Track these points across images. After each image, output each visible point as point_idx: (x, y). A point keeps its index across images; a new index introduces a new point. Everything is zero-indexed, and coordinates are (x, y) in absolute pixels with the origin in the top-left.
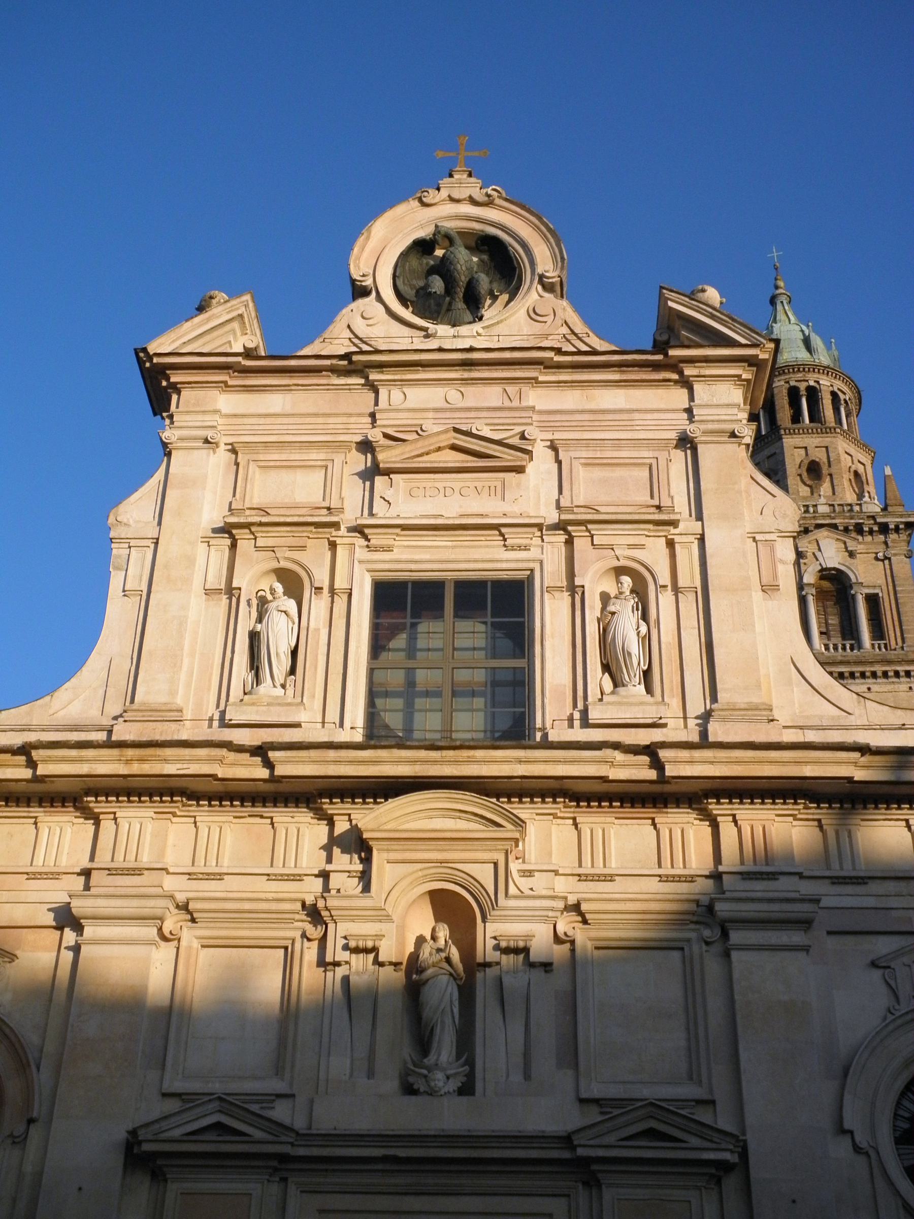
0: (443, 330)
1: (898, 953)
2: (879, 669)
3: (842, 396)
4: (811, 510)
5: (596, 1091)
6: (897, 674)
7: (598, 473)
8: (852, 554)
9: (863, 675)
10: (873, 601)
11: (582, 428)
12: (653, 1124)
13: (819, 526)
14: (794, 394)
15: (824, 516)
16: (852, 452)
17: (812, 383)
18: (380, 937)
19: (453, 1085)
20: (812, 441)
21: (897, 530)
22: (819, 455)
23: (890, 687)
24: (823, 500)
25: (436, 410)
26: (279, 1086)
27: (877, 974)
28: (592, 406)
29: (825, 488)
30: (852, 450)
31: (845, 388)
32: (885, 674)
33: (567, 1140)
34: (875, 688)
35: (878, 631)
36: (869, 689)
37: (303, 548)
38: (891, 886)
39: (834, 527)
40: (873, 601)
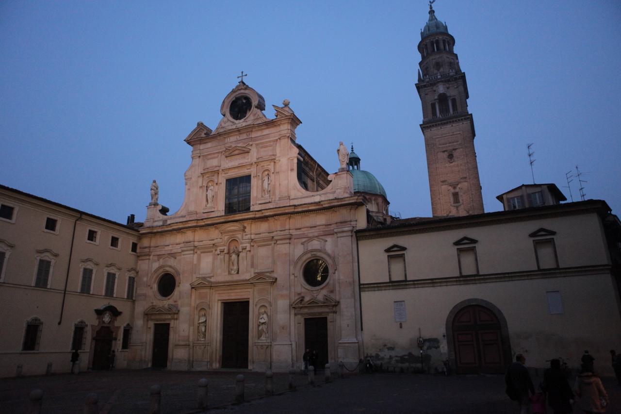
0: (237, 122)
1: (305, 242)
2: (454, 120)
3: (446, 40)
5: (256, 271)
7: (263, 149)
8: (448, 88)
9: (450, 122)
10: (454, 100)
11: (261, 139)
12: (261, 276)
13: (438, 82)
14: (432, 43)
15: (440, 78)
16: (449, 56)
18: (224, 249)
19: (236, 272)
20: (438, 56)
21: (459, 79)
23: (457, 124)
24: (439, 74)
25: (235, 141)
26: (212, 275)
27: (302, 246)
28: (263, 134)
29: (441, 70)
30: (449, 56)
31: (447, 37)
32: (456, 121)
33: (249, 280)
34: (453, 125)
36: (452, 126)
37: (213, 176)
38: (305, 229)
39: (442, 81)
40: (454, 100)
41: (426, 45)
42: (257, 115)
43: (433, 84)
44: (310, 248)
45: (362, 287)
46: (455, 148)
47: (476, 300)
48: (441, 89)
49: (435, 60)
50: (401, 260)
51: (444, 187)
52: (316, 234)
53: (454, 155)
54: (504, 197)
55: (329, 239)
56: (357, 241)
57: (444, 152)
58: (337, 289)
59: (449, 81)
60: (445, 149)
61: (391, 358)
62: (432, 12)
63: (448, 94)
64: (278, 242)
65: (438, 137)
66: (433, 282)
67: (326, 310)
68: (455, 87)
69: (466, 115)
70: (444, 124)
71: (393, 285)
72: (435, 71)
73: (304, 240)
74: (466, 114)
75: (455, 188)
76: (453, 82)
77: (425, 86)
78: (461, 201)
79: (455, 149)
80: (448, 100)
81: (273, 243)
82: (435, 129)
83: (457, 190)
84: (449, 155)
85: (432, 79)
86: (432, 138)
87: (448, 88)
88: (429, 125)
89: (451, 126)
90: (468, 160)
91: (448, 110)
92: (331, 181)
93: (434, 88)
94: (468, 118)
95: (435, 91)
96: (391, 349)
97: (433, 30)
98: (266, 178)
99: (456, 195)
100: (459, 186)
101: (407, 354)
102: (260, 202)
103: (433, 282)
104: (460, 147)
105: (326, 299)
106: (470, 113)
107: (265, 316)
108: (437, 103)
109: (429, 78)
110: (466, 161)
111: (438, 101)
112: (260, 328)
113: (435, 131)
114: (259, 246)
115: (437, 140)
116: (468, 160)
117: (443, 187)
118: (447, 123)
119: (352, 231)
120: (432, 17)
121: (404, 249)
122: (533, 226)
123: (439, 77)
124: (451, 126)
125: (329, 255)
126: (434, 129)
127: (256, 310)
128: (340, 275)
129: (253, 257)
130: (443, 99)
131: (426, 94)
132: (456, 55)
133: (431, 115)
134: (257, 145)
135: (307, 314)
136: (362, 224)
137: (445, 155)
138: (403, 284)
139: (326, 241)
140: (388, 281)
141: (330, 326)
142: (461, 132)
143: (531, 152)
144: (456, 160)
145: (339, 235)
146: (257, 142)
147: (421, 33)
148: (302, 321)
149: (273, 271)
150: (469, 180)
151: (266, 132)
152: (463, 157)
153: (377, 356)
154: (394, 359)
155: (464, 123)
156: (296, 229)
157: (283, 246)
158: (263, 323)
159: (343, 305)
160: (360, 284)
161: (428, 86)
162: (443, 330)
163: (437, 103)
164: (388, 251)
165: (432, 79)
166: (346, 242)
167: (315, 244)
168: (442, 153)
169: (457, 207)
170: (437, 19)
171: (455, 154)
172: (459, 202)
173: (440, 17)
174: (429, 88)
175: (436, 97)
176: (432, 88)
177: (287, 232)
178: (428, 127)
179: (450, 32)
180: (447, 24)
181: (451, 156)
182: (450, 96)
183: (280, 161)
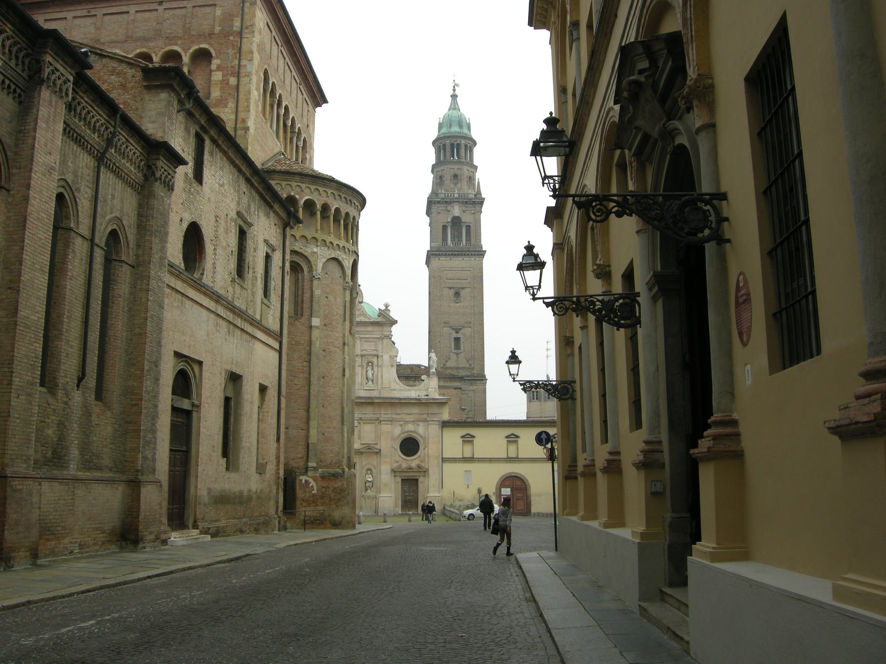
2: (467, 253)
3: (469, 145)
5: (363, 442)
6: (472, 254)
7: (367, 343)
8: (464, 211)
9: (462, 255)
10: (468, 227)
13: (454, 202)
14: (452, 145)
15: (457, 198)
20: (456, 167)
22: (457, 172)
23: (469, 259)
29: (459, 185)
31: (470, 142)
34: (465, 259)
39: (459, 202)
41: (444, 145)
42: (361, 311)
43: (448, 202)
44: (406, 430)
45: (444, 460)
46: (463, 286)
47: (515, 473)
48: (456, 211)
49: (453, 170)
51: (446, 330)
52: (412, 420)
53: (461, 295)
55: (421, 424)
56: (442, 427)
57: (450, 288)
58: (426, 460)
59: (466, 203)
60: (451, 286)
61: (460, 506)
62: (454, 97)
63: (463, 220)
64: (382, 423)
66: (490, 460)
67: (418, 474)
68: (472, 212)
70: (455, 255)
71: (465, 460)
72: (452, 186)
73: (402, 423)
74: (480, 250)
75: (457, 332)
76: (470, 206)
77: (439, 202)
78: (462, 348)
79: (463, 288)
80: (461, 227)
81: (377, 422)
82: (444, 259)
83: (459, 335)
84: (455, 294)
85: (448, 196)
87: (464, 211)
88: (438, 253)
90: (475, 303)
92: (424, 380)
93: (449, 208)
94: (482, 255)
95: (449, 211)
96: (462, 500)
97: (455, 129)
98: (369, 368)
99: (457, 340)
100: (462, 331)
101: (470, 503)
102: (365, 388)
103: (490, 460)
104: (469, 286)
105: (419, 467)
106: (483, 250)
107: (370, 476)
108: (449, 227)
109: (445, 194)
112: (367, 485)
114: (364, 423)
115: (445, 272)
116: (475, 303)
117: (445, 328)
118: (458, 255)
119: (439, 421)
121: (474, 437)
125: (421, 436)
127: (364, 471)
128: (429, 451)
129: (360, 431)
130: (456, 221)
131: (439, 213)
132: (476, 168)
133: (441, 240)
134: (360, 338)
135: (404, 476)
137: (452, 292)
138: (471, 460)
139: (419, 425)
141: (420, 485)
142: (472, 269)
143: (549, 348)
144: (461, 299)
145: (429, 423)
146: (361, 336)
148: (399, 480)
149: (377, 444)
150: (472, 326)
151: (370, 329)
152: (470, 298)
153: (451, 506)
154: (462, 507)
156: (396, 414)
157: (386, 426)
158: (370, 481)
159: (430, 472)
161: (442, 203)
162: (494, 490)
163: (449, 227)
164: (463, 437)
165: (448, 196)
166: (434, 429)
167: (410, 427)
168: (448, 289)
169: (457, 354)
170: (459, 110)
171: (462, 293)
172: (460, 349)
173: (467, 110)
174: (442, 205)
175: (449, 220)
176: (446, 207)
177: (389, 416)
178: (436, 254)
179: (475, 134)
180: (471, 122)
181: (457, 294)
182: (465, 222)
183: (382, 356)
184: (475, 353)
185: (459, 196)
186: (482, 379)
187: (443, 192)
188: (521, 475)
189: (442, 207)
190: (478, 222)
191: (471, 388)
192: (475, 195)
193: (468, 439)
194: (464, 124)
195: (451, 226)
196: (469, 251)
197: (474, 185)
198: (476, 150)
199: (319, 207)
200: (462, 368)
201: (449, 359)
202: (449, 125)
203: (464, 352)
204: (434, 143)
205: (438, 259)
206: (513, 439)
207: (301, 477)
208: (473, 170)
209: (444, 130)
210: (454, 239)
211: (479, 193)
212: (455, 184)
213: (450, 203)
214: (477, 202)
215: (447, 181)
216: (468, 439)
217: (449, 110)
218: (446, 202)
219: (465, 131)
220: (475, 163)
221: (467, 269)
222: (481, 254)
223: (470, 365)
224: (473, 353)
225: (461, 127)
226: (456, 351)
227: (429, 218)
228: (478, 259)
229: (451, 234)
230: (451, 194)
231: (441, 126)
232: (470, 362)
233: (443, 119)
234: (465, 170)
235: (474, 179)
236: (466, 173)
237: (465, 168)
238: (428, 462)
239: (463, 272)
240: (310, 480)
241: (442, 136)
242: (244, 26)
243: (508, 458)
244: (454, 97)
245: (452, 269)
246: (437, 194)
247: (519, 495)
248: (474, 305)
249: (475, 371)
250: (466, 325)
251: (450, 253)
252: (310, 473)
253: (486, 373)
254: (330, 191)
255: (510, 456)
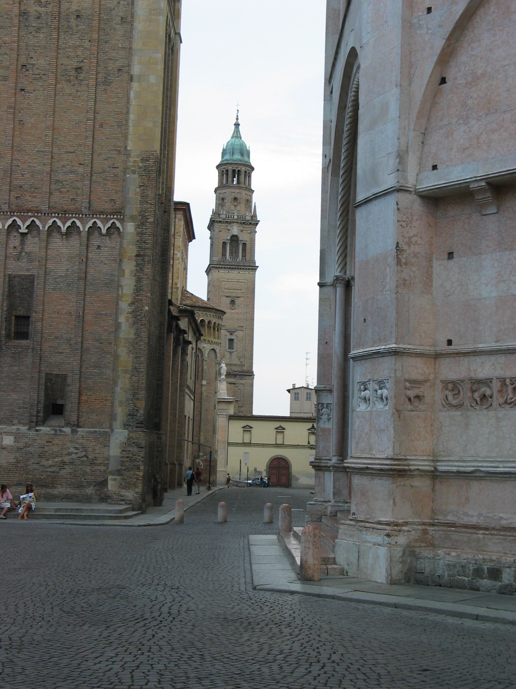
3: (248, 172)
4: (232, 216)
6: (246, 269)
8: (242, 231)
10: (244, 245)
14: (234, 171)
17: (239, 169)
23: (244, 272)
29: (238, 208)
31: (249, 169)
34: (241, 272)
35: (244, 255)
41: (227, 171)
45: (229, 444)
46: (239, 295)
48: (235, 230)
49: (233, 194)
50: (249, 433)
53: (236, 303)
54: (291, 391)
56: (229, 420)
57: (227, 297)
59: (244, 223)
62: (237, 125)
63: (241, 238)
65: (224, 280)
68: (249, 232)
69: (253, 266)
71: (244, 444)
72: (232, 207)
75: (231, 334)
77: (220, 222)
78: (235, 348)
79: (238, 297)
82: (223, 271)
83: (233, 337)
86: (219, 280)
87: (242, 231)
89: (238, 272)
90: (248, 311)
91: (237, 252)
95: (229, 230)
97: (237, 157)
99: (231, 341)
100: (236, 333)
109: (226, 215)
110: (245, 312)
111: (230, 242)
113: (223, 274)
115: (223, 283)
116: (248, 311)
119: (226, 415)
120: (237, 133)
121: (251, 428)
122: (309, 425)
123: (236, 217)
124: (238, 272)
126: (222, 271)
130: (234, 239)
132: (253, 191)
136: (231, 412)
138: (249, 444)
140: (242, 442)
145: (219, 416)
147: (224, 150)
152: (243, 306)
155: (250, 273)
160: (228, 443)
163: (228, 244)
164: (243, 427)
168: (225, 298)
169: (231, 353)
170: (241, 138)
171: (237, 301)
172: (233, 349)
174: (223, 225)
175: (229, 238)
176: (227, 226)
179: (253, 162)
184: (246, 353)
185: (238, 217)
186: (250, 374)
187: (224, 213)
188: (286, 457)
189: (223, 226)
190: (253, 241)
191: (241, 382)
192: (252, 217)
193: (247, 429)
194: (245, 153)
195: (230, 243)
196: (245, 266)
197: (251, 207)
198: (253, 174)
199: (207, 323)
200: (234, 365)
201: (224, 356)
202: (231, 153)
203: (236, 351)
204: (218, 167)
205: (218, 271)
206: (280, 430)
207: (197, 460)
208: (250, 194)
209: (227, 157)
210: (232, 254)
211: (254, 216)
212: (236, 206)
213: (230, 222)
214: (253, 222)
215: (228, 203)
216: (247, 429)
217: (232, 137)
218: (227, 222)
219: (246, 158)
220: (253, 187)
221: (242, 281)
222: (254, 268)
223: (241, 362)
224: (244, 353)
225: (242, 155)
226: (230, 350)
227: (210, 232)
228: (252, 273)
229: (230, 250)
230: (231, 215)
231: (224, 153)
232: (242, 360)
233: (227, 146)
234: (244, 194)
235: (251, 202)
236: (245, 197)
237: (244, 192)
238: (217, 445)
239: (238, 283)
240: (201, 461)
241: (225, 162)
242: (176, 232)
243: (276, 444)
244: (237, 125)
245: (229, 280)
246: (219, 215)
247: (282, 472)
248: (246, 313)
249: (245, 368)
250: (239, 329)
251: (229, 267)
252: (200, 458)
253: (254, 370)
254: (212, 314)
255: (278, 443)
